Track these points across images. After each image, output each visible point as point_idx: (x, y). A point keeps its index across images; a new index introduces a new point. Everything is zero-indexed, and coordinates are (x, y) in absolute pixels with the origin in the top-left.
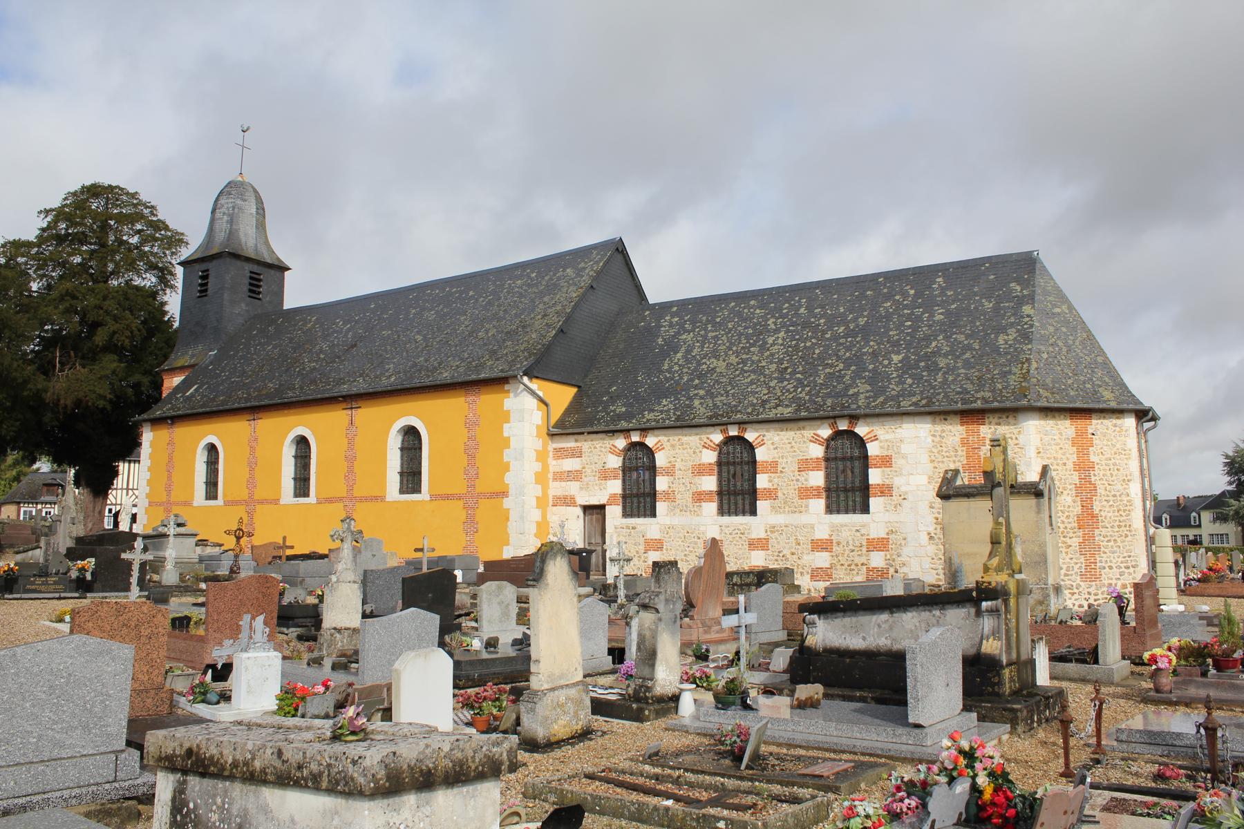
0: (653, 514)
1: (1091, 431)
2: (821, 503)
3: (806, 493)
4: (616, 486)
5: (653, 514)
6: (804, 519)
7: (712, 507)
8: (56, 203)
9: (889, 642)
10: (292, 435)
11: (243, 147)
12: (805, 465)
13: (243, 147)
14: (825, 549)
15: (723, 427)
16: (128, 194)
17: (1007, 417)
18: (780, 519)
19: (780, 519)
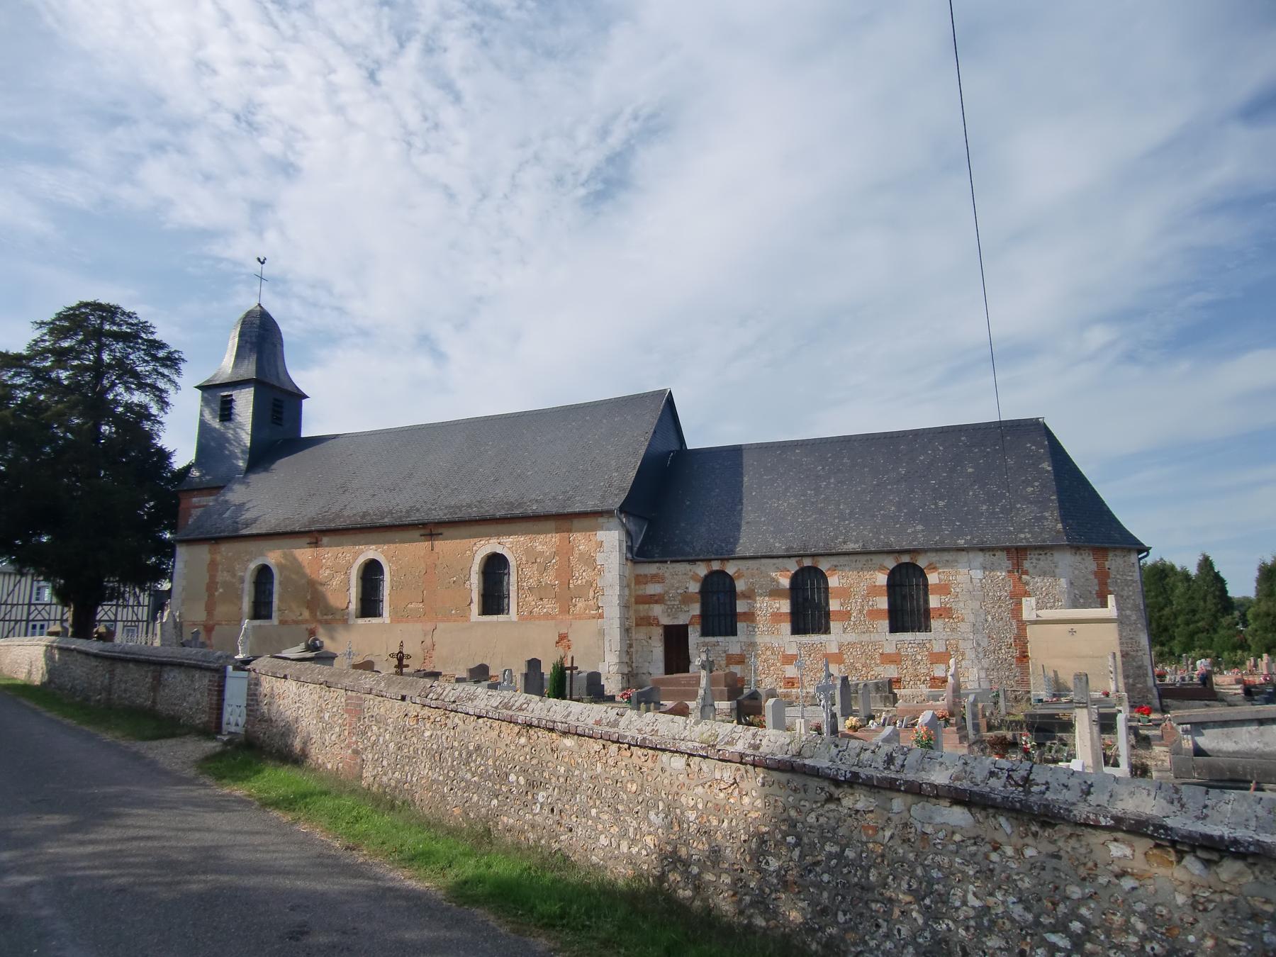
0: (734, 633)
1: (1107, 567)
2: (885, 624)
3: (874, 614)
4: (696, 609)
5: (734, 633)
6: (875, 637)
7: (786, 627)
8: (49, 317)
9: (1261, 746)
10: (362, 560)
11: (261, 278)
12: (873, 591)
13: (261, 278)
14: (892, 662)
15: (798, 559)
16: (124, 313)
17: (1046, 554)
18: (851, 637)
19: (851, 637)
